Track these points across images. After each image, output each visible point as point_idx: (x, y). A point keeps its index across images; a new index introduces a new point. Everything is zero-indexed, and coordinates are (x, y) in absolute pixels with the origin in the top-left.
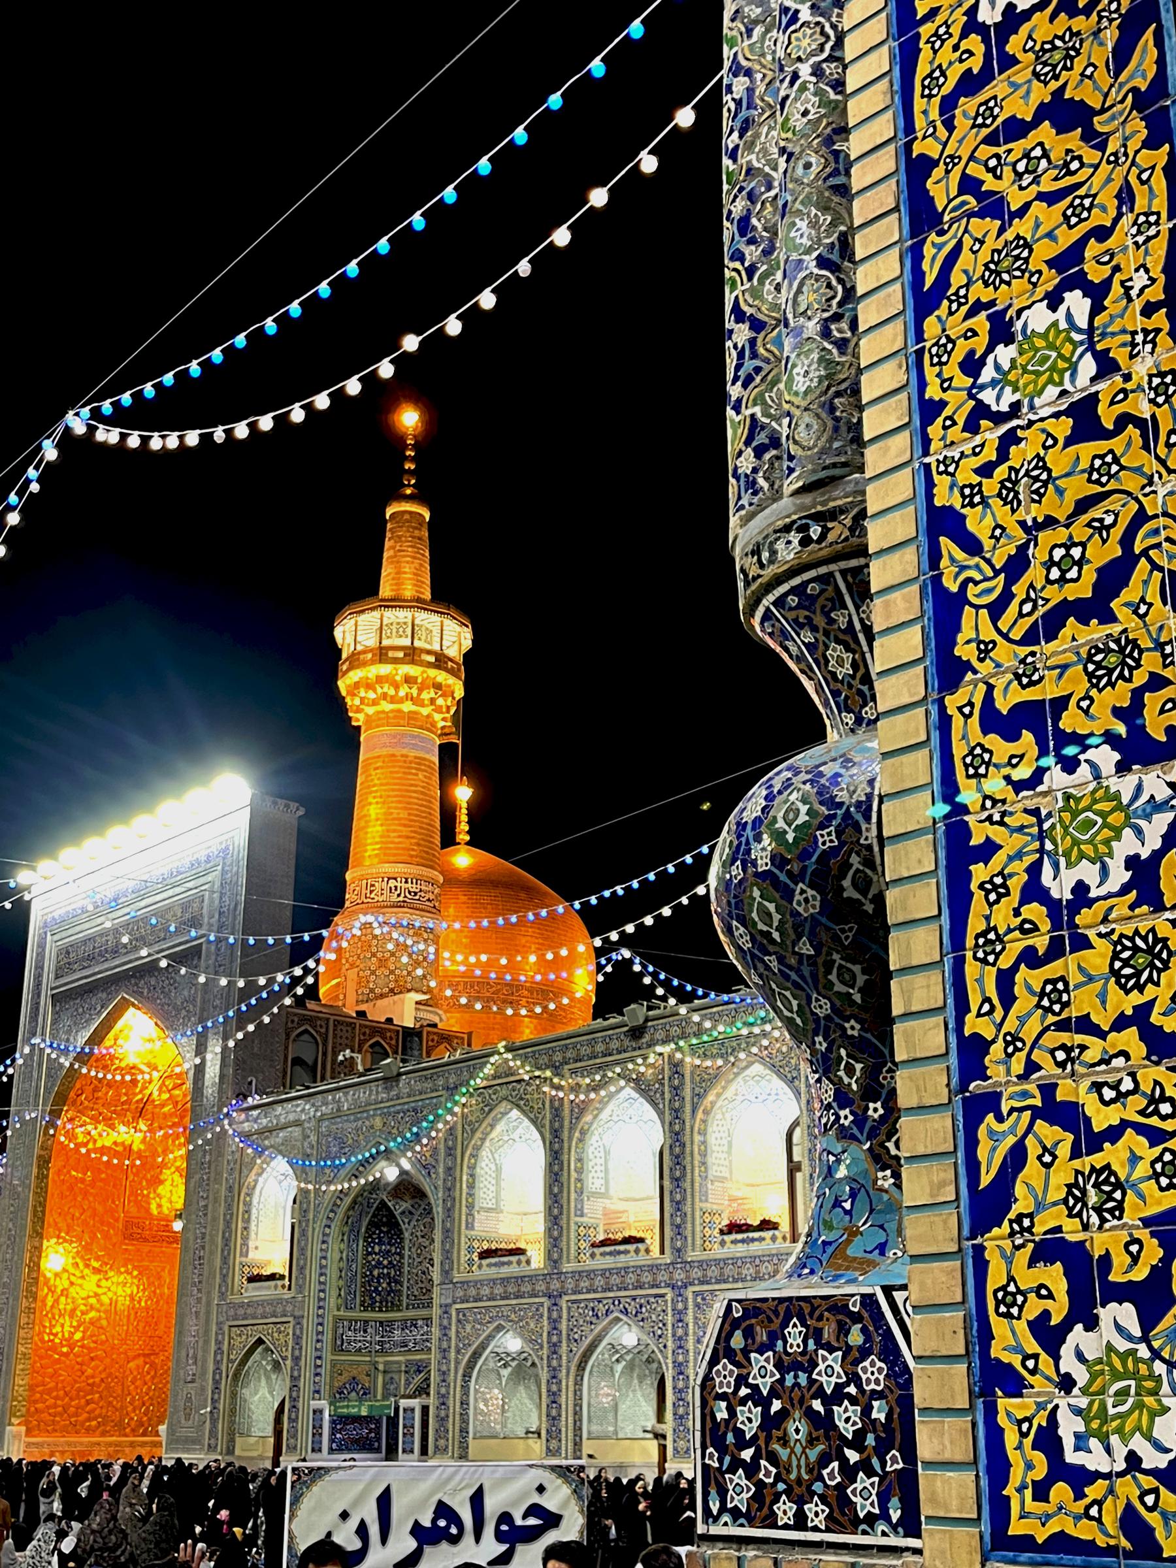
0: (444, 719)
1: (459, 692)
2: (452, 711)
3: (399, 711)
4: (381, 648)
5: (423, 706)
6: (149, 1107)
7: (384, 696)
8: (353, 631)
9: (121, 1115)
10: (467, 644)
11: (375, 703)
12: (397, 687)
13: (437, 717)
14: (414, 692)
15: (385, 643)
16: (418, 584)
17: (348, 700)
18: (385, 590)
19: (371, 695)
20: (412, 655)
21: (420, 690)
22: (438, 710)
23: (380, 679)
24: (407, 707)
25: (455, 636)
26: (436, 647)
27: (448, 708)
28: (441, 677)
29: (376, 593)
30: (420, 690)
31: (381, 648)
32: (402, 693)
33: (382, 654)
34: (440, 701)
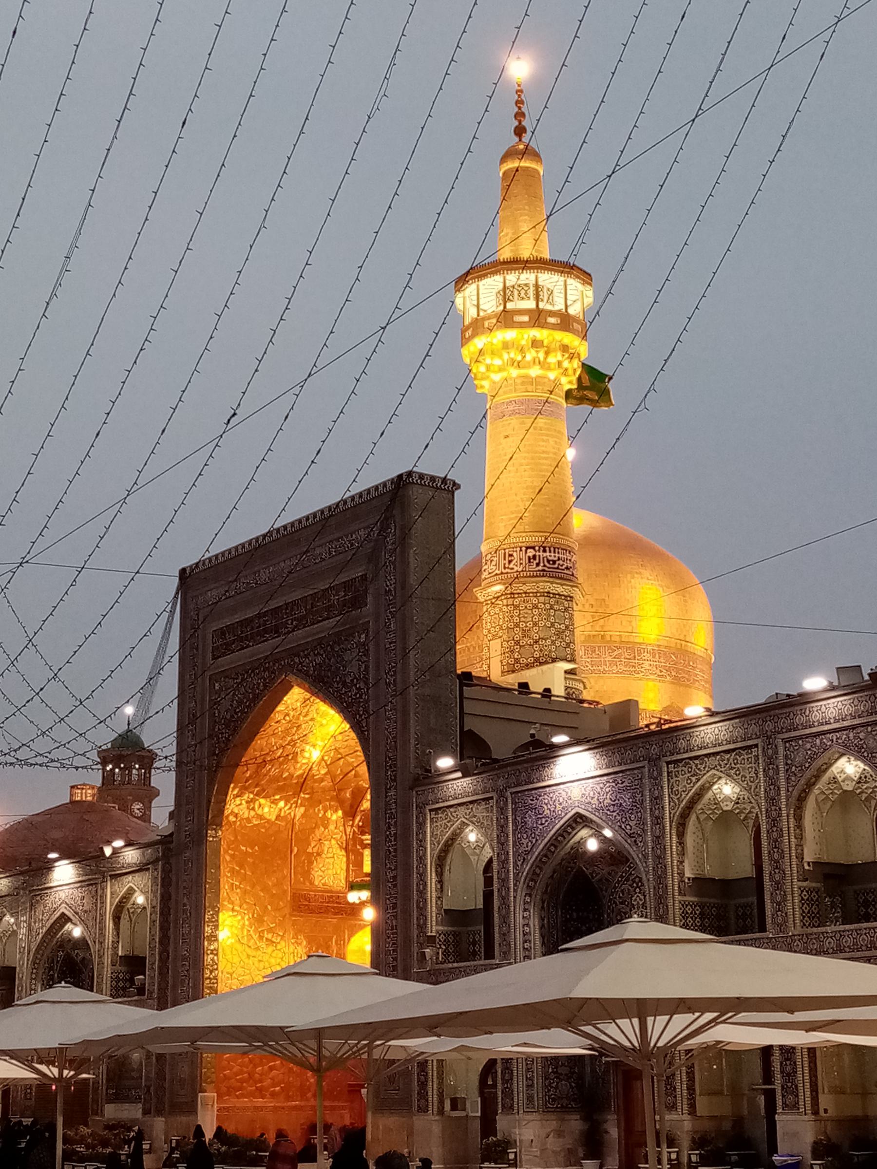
0: (570, 382)
2: (578, 373)
3: (526, 377)
5: (549, 369)
6: (308, 782)
7: (513, 362)
9: (280, 790)
11: (501, 369)
12: (522, 350)
13: (564, 380)
14: (541, 355)
15: (509, 306)
19: (497, 362)
21: (547, 353)
22: (565, 372)
23: (506, 346)
24: (535, 372)
26: (559, 306)
27: (575, 370)
30: (547, 353)
32: (529, 357)
33: (506, 319)
34: (566, 364)
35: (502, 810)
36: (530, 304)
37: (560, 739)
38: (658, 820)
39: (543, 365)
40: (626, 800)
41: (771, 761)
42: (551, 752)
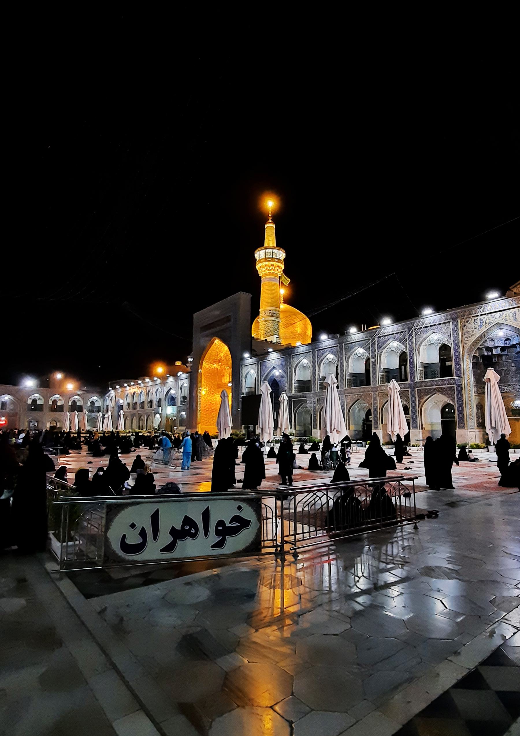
1: (283, 268)
4: (266, 258)
7: (267, 269)
8: (259, 254)
10: (285, 257)
11: (265, 271)
16: (273, 243)
17: (259, 271)
18: (266, 245)
20: (272, 259)
23: (266, 265)
24: (272, 271)
25: (282, 254)
28: (279, 264)
29: (263, 245)
31: (266, 258)
33: (266, 259)
35: (258, 366)
36: (271, 257)
37: (270, 350)
38: (290, 368)
39: (274, 270)
40: (284, 364)
41: (314, 355)
42: (268, 353)
